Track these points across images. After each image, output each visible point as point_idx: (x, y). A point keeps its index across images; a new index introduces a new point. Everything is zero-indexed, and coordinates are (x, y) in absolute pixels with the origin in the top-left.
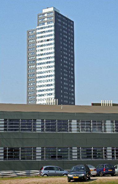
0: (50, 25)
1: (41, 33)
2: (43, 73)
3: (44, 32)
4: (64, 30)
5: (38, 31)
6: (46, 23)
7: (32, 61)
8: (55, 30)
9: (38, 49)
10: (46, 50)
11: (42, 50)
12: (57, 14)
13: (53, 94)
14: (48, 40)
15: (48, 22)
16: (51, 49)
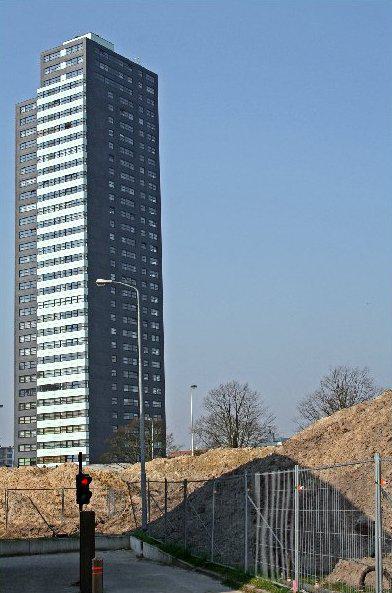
0: (72, 80)
1: (50, 105)
2: (49, 404)
3: (57, 102)
4: (122, 109)
5: (41, 102)
6: (63, 77)
7: (26, 194)
8: (89, 93)
9: (40, 258)
10: (64, 152)
11: (52, 156)
12: (97, 53)
13: (83, 427)
14: (68, 126)
15: (69, 74)
16: (77, 216)
